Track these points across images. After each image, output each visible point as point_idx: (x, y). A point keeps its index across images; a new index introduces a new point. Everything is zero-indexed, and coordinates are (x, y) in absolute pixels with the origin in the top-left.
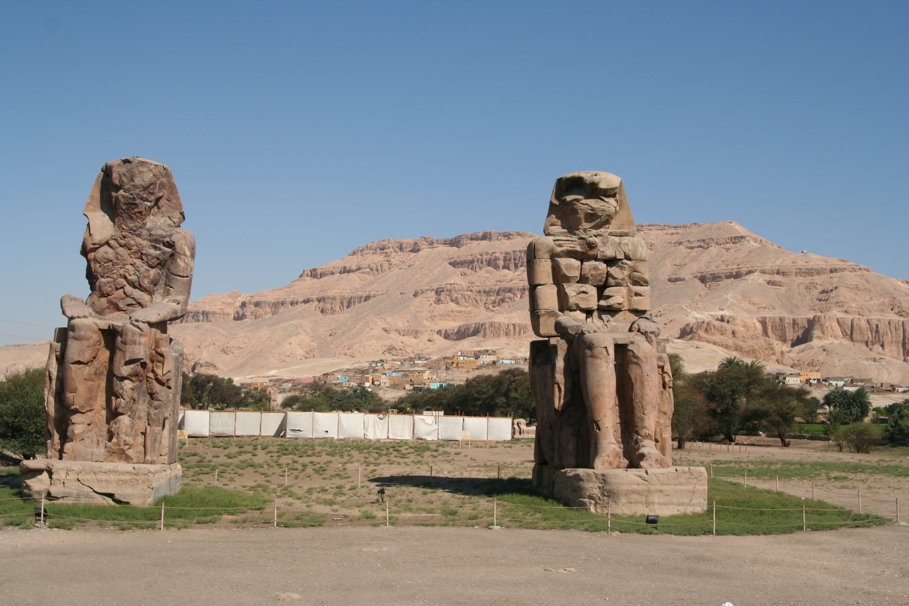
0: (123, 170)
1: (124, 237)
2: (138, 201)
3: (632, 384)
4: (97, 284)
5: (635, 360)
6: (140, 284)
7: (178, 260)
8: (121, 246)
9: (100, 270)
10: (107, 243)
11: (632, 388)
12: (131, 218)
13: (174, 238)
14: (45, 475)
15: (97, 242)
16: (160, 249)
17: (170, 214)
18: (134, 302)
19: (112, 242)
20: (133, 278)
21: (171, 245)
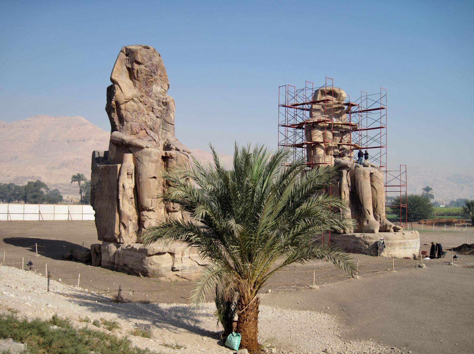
0: (144, 51)
1: (143, 96)
2: (153, 74)
3: (377, 192)
4: (129, 125)
5: (378, 181)
6: (154, 128)
7: (171, 114)
8: (141, 102)
9: (130, 116)
10: (132, 99)
11: (377, 194)
12: (147, 84)
13: (168, 100)
14: (167, 256)
15: (128, 98)
16: (161, 106)
17: (162, 85)
18: (152, 139)
19: (136, 99)
20: (150, 123)
21: (166, 104)
